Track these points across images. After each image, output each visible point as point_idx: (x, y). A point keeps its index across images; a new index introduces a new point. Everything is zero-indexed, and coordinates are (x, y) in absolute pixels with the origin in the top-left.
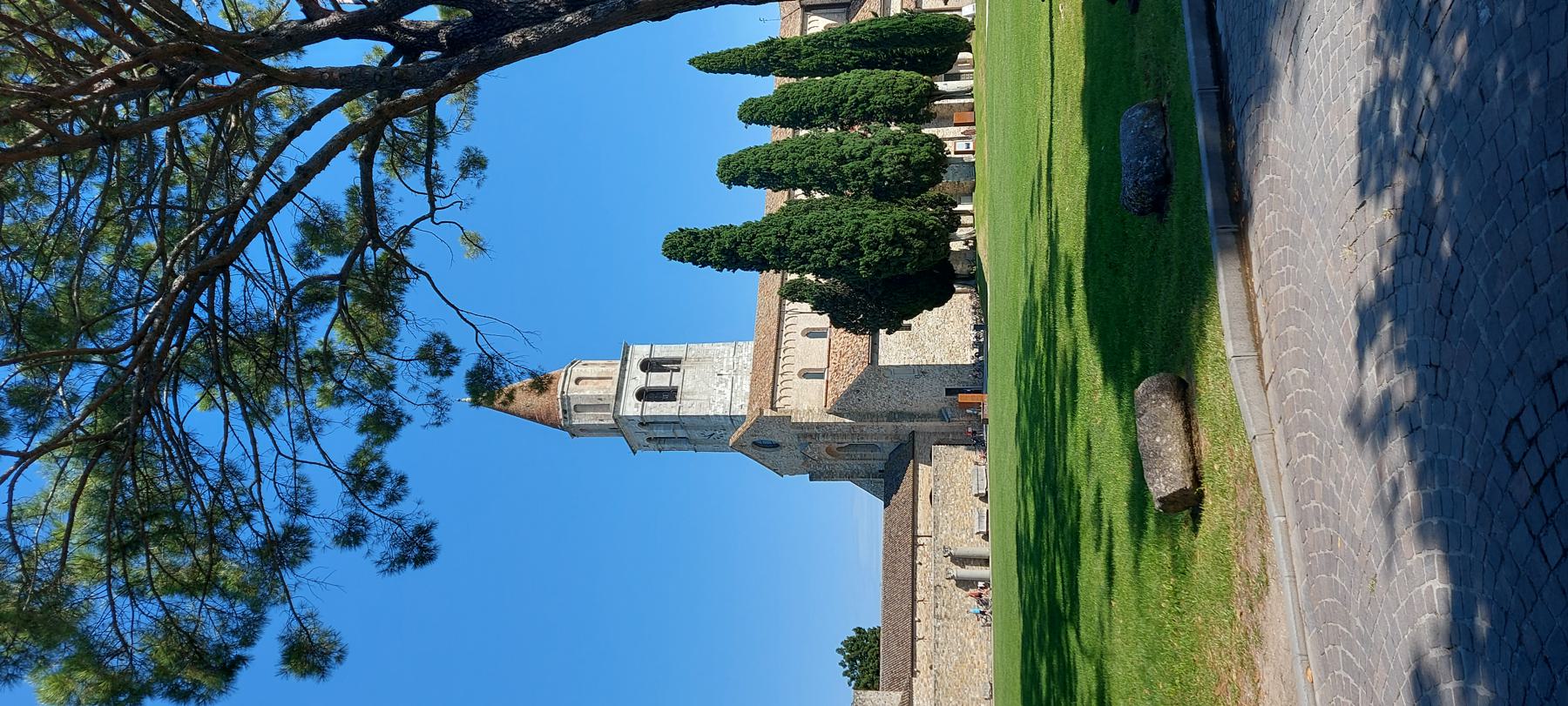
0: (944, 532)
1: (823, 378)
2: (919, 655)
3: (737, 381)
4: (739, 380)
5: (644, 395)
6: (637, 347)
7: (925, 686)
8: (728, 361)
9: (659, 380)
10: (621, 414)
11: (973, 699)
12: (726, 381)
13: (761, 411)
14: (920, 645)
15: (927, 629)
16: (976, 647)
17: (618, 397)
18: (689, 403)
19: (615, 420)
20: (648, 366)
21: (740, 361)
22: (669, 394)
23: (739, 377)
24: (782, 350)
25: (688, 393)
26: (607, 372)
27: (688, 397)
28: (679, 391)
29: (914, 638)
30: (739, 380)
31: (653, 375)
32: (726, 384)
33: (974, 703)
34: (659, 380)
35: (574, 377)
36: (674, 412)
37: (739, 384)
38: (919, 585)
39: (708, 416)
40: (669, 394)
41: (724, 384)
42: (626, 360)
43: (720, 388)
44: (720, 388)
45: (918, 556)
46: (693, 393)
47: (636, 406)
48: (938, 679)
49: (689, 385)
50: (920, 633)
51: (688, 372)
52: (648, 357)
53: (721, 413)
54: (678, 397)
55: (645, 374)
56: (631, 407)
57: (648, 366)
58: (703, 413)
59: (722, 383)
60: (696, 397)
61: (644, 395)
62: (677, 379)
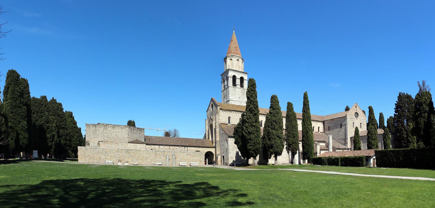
0: (180, 154)
1: (229, 123)
2: (155, 146)
4: (238, 103)
5: (234, 77)
6: (247, 76)
7: (144, 147)
8: (243, 100)
9: (238, 82)
11: (133, 160)
13: (219, 106)
14: (157, 147)
15: (162, 148)
16: (148, 161)
17: (234, 70)
19: (228, 69)
20: (242, 79)
21: (243, 103)
22: (234, 84)
24: (236, 112)
25: (235, 89)
26: (240, 68)
27: (234, 90)
29: (159, 145)
30: (238, 103)
31: (239, 80)
32: (238, 99)
33: (132, 160)
34: (238, 82)
38: (174, 147)
39: (229, 94)
40: (234, 84)
42: (243, 73)
43: (236, 98)
45: (182, 147)
46: (235, 90)
47: (231, 75)
48: (139, 151)
49: (237, 89)
50: (161, 147)
51: (240, 89)
52: (244, 79)
54: (234, 87)
55: (240, 78)
56: (231, 74)
57: (242, 79)
58: (230, 93)
60: (234, 91)
61: (234, 77)
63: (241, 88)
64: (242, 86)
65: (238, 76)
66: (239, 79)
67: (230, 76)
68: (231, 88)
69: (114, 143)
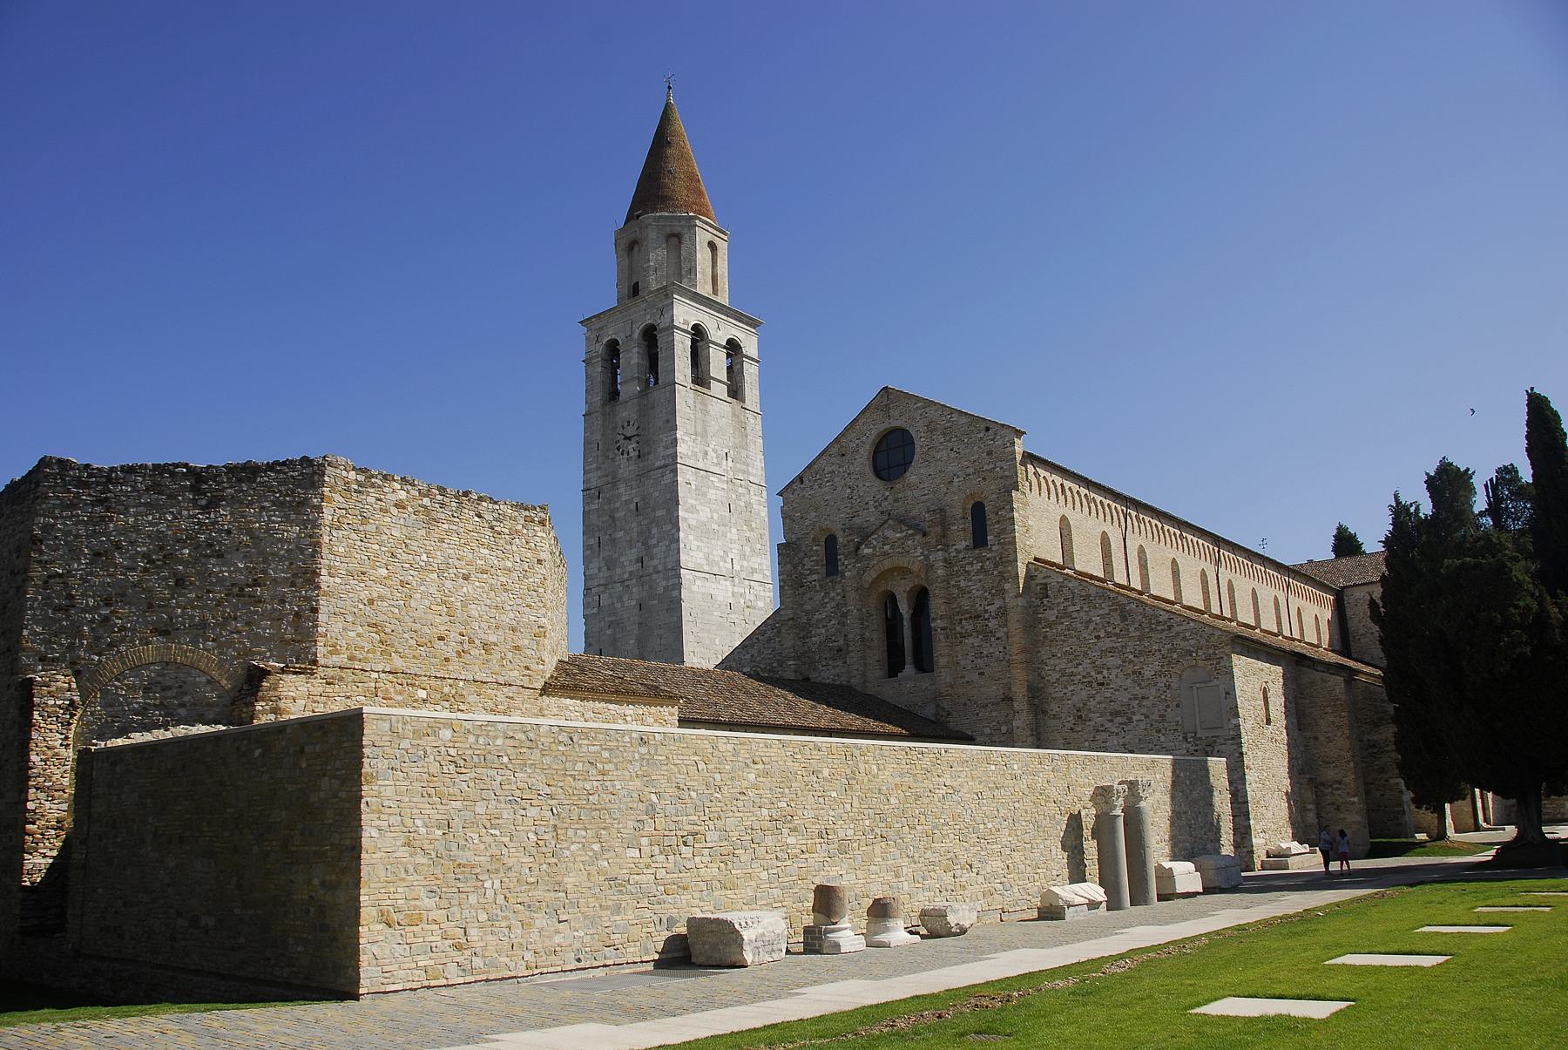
3: (720, 481)
9: (718, 362)
10: (675, 296)
12: (718, 464)
18: (691, 402)
23: (725, 486)
28: (705, 390)
31: (722, 354)
34: (718, 362)
35: (717, 241)
36: (679, 378)
37: (717, 484)
41: (715, 460)
44: (711, 453)
47: (686, 322)
53: (679, 449)
57: (733, 347)
59: (717, 457)
60: (699, 414)
62: (719, 389)
63: (729, 399)
64: (735, 392)
65: (720, 331)
66: (724, 347)
67: (681, 326)
68: (685, 395)
69: (422, 694)
